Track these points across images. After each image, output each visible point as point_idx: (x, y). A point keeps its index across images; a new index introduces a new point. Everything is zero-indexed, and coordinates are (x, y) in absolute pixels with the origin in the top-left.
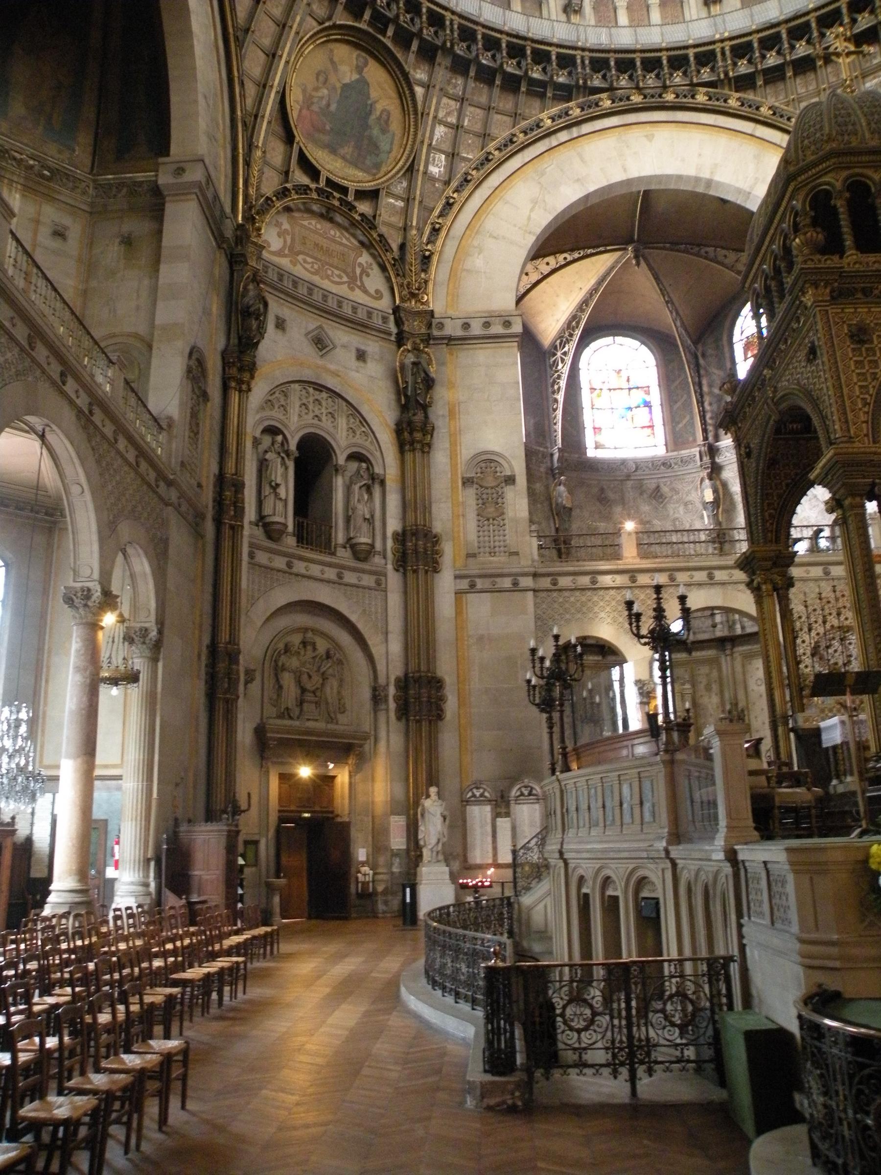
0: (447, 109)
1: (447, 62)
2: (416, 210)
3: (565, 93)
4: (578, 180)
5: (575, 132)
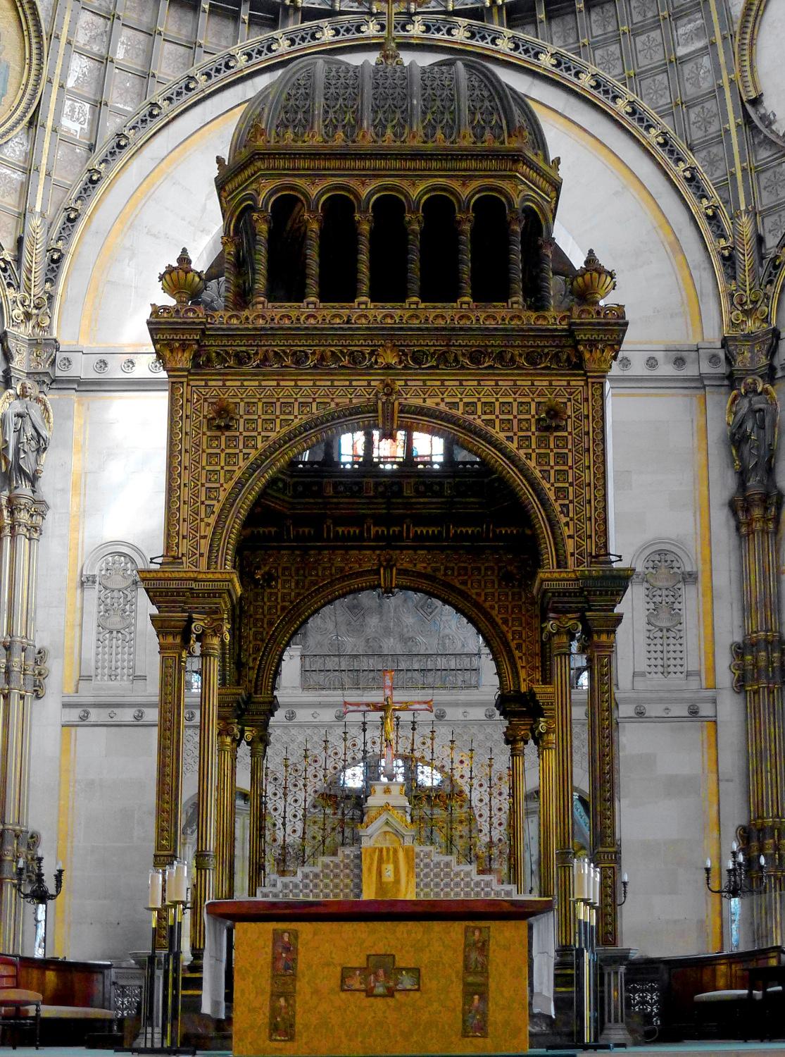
2: (41, 188)
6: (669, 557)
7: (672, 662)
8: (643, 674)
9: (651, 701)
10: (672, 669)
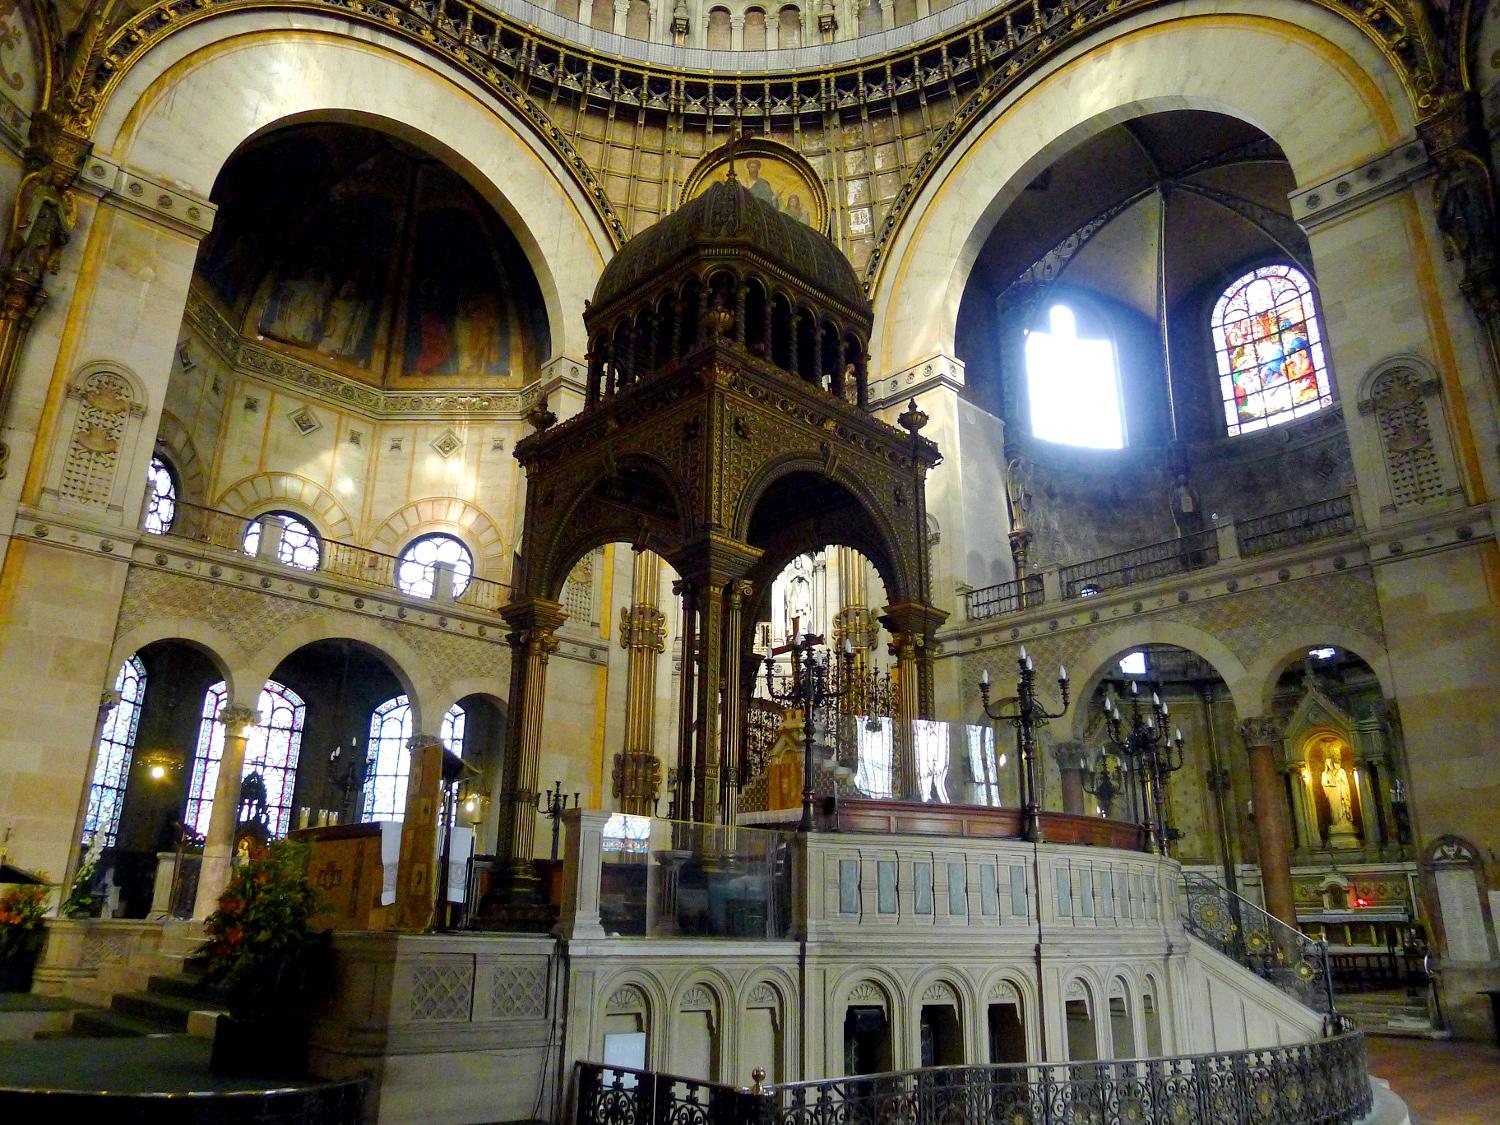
0: (852, 162)
1: (836, 120)
3: (971, 80)
4: (996, 172)
5: (990, 117)
6: (1402, 374)
7: (1425, 485)
8: (1394, 508)
9: (1405, 535)
10: (1428, 493)
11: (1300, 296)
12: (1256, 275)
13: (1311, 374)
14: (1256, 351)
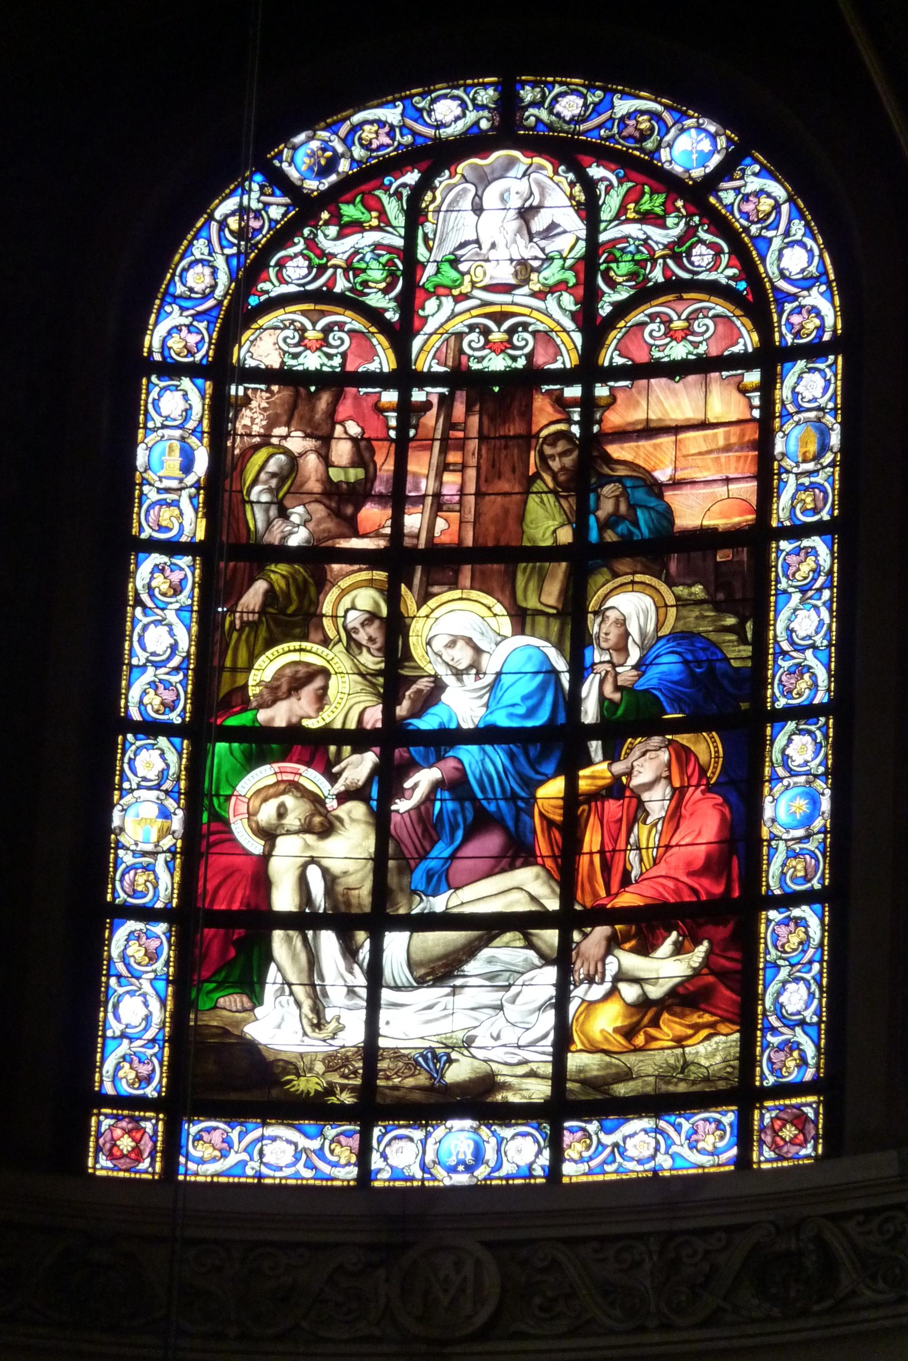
11: (771, 358)
12: (508, 107)
13: (723, 909)
14: (395, 627)
